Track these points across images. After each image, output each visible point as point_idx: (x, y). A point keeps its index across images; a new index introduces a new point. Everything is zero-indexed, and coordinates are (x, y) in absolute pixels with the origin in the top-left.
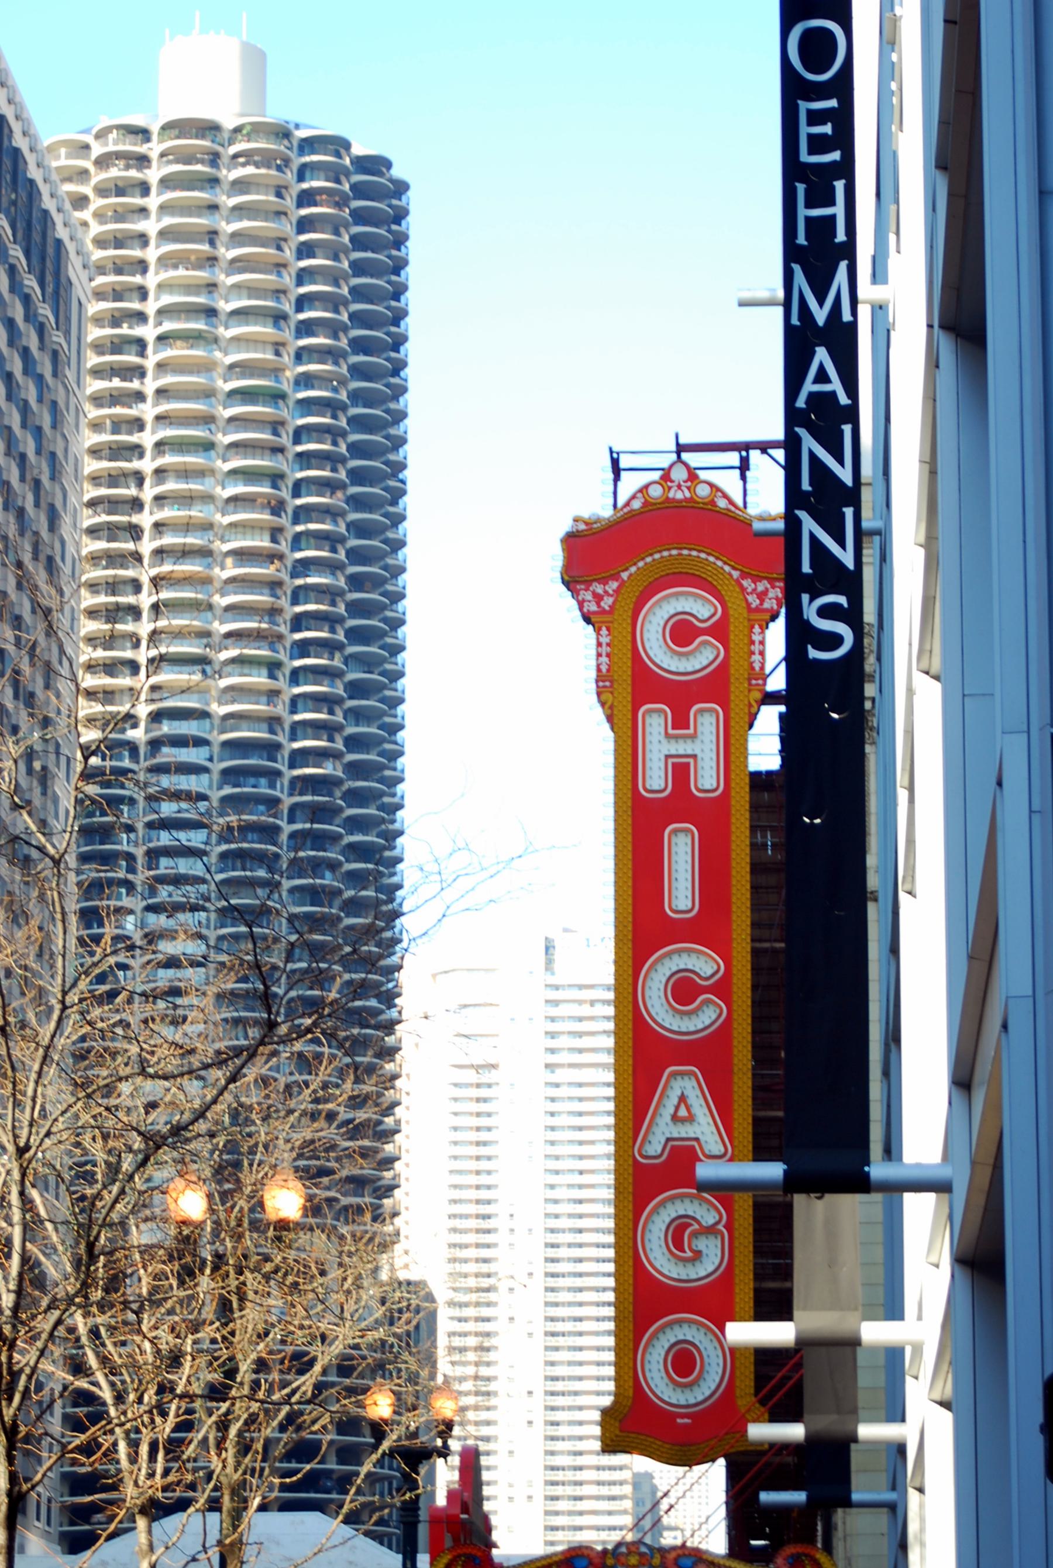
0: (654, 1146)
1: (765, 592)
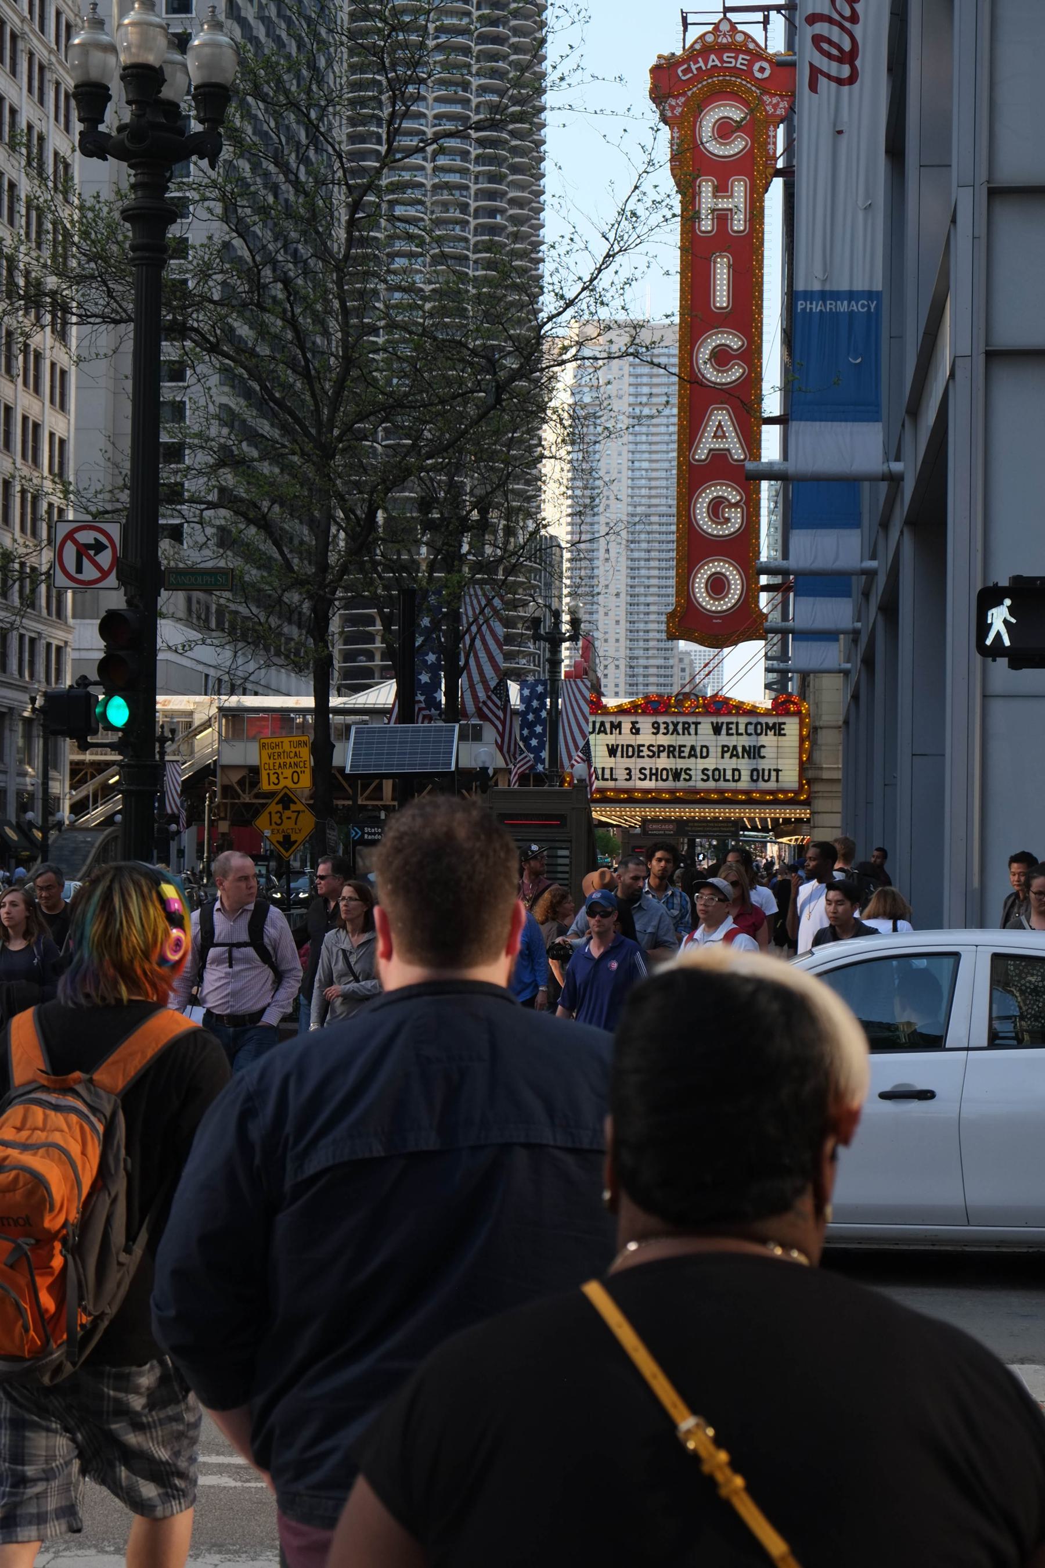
0: (701, 454)
1: (778, 104)
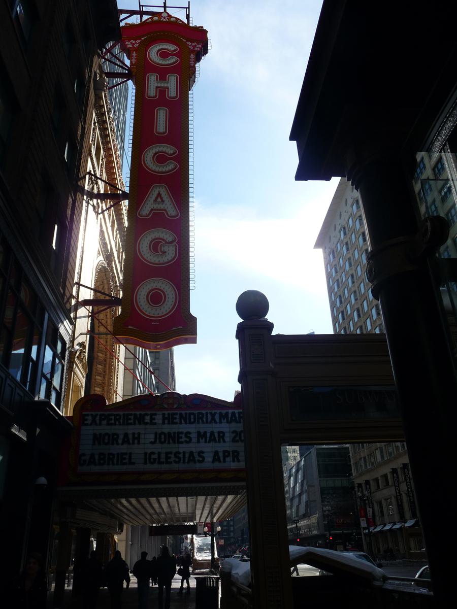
1: (196, 45)
